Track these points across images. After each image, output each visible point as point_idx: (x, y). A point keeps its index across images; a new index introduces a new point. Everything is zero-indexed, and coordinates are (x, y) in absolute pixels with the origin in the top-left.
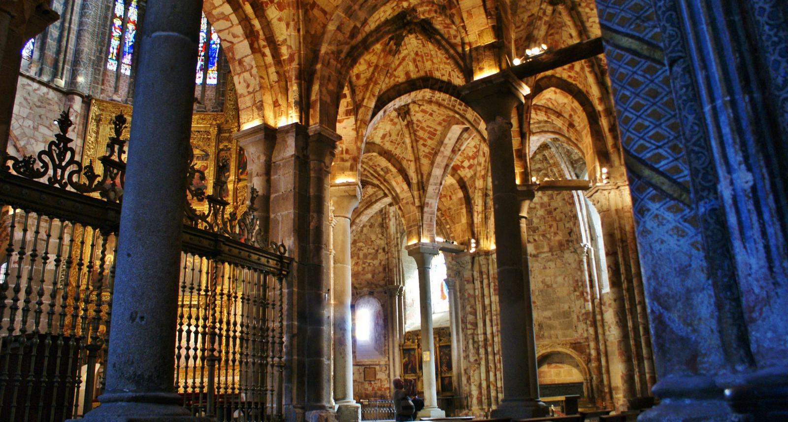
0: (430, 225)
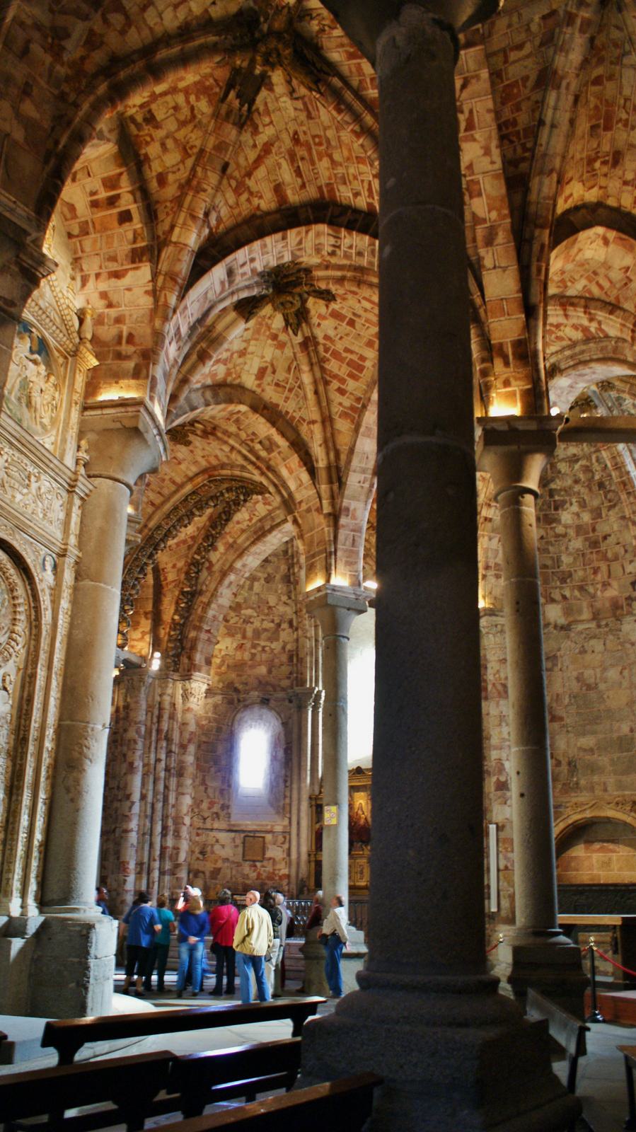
0: (352, 553)
